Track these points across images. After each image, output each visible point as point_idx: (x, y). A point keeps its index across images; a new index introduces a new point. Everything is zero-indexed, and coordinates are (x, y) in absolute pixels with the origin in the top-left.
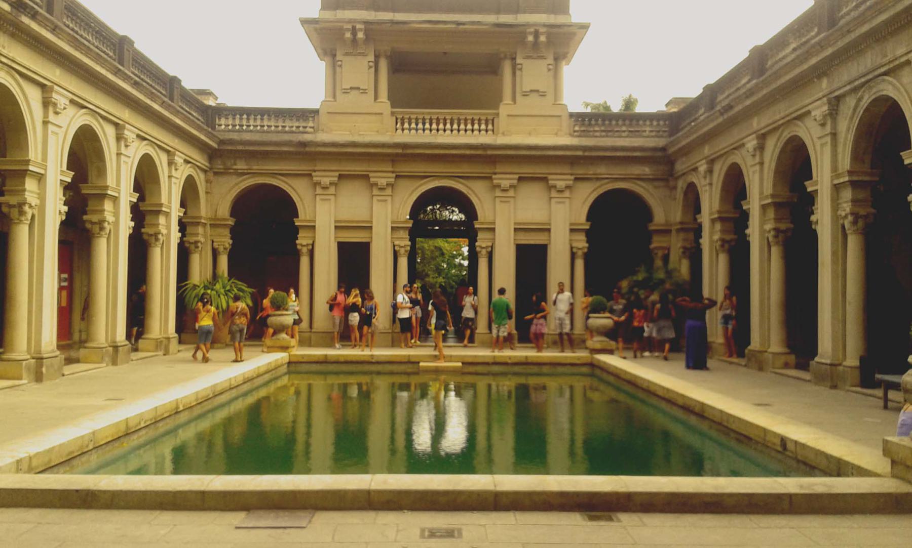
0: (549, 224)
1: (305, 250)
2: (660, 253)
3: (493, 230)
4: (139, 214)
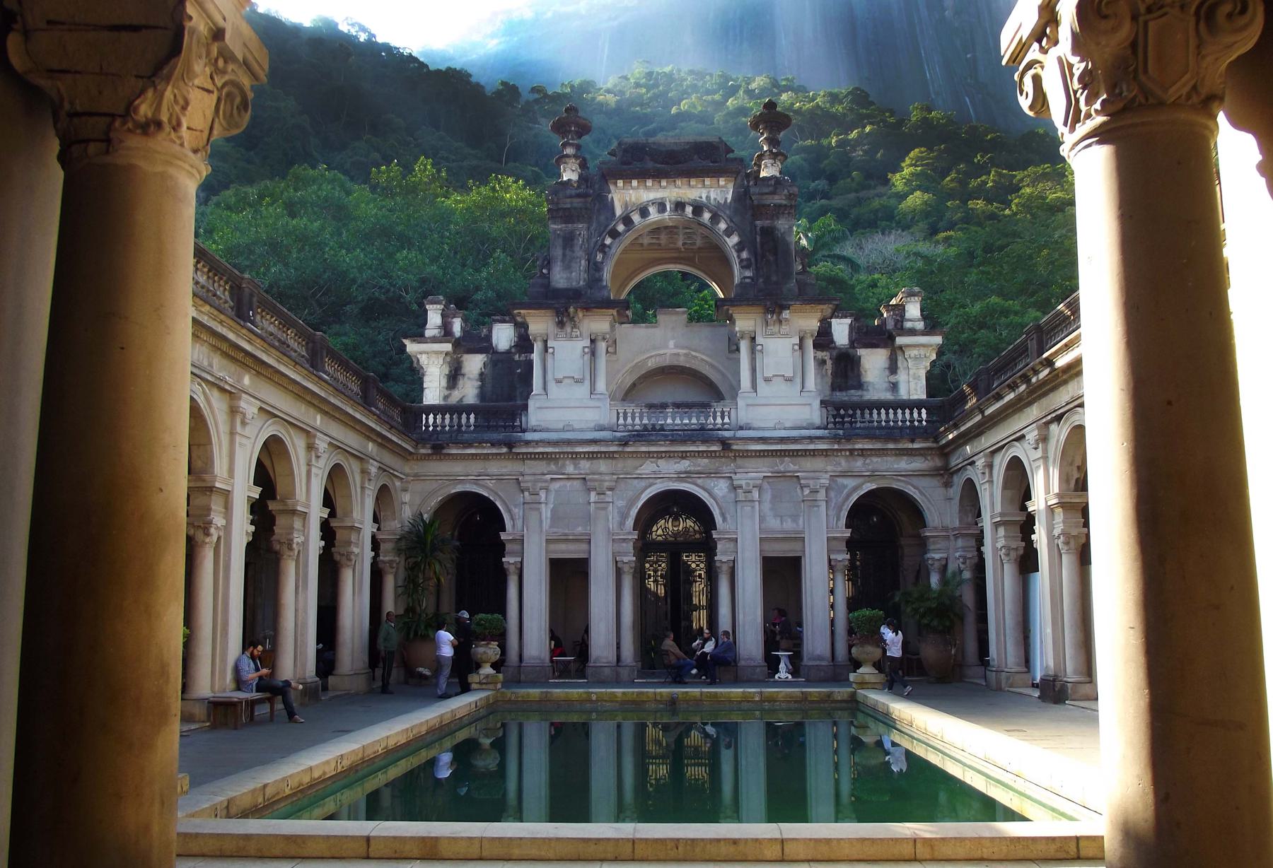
0: (803, 532)
1: (512, 569)
2: (937, 565)
3: (736, 540)
4: (262, 513)
